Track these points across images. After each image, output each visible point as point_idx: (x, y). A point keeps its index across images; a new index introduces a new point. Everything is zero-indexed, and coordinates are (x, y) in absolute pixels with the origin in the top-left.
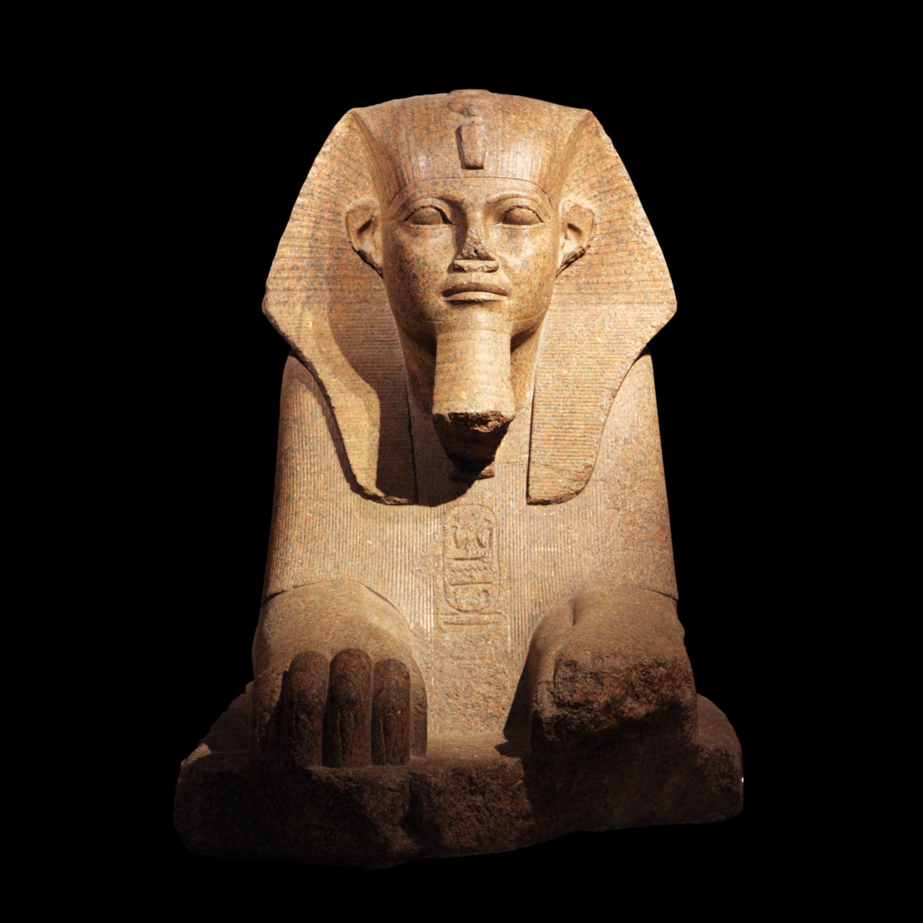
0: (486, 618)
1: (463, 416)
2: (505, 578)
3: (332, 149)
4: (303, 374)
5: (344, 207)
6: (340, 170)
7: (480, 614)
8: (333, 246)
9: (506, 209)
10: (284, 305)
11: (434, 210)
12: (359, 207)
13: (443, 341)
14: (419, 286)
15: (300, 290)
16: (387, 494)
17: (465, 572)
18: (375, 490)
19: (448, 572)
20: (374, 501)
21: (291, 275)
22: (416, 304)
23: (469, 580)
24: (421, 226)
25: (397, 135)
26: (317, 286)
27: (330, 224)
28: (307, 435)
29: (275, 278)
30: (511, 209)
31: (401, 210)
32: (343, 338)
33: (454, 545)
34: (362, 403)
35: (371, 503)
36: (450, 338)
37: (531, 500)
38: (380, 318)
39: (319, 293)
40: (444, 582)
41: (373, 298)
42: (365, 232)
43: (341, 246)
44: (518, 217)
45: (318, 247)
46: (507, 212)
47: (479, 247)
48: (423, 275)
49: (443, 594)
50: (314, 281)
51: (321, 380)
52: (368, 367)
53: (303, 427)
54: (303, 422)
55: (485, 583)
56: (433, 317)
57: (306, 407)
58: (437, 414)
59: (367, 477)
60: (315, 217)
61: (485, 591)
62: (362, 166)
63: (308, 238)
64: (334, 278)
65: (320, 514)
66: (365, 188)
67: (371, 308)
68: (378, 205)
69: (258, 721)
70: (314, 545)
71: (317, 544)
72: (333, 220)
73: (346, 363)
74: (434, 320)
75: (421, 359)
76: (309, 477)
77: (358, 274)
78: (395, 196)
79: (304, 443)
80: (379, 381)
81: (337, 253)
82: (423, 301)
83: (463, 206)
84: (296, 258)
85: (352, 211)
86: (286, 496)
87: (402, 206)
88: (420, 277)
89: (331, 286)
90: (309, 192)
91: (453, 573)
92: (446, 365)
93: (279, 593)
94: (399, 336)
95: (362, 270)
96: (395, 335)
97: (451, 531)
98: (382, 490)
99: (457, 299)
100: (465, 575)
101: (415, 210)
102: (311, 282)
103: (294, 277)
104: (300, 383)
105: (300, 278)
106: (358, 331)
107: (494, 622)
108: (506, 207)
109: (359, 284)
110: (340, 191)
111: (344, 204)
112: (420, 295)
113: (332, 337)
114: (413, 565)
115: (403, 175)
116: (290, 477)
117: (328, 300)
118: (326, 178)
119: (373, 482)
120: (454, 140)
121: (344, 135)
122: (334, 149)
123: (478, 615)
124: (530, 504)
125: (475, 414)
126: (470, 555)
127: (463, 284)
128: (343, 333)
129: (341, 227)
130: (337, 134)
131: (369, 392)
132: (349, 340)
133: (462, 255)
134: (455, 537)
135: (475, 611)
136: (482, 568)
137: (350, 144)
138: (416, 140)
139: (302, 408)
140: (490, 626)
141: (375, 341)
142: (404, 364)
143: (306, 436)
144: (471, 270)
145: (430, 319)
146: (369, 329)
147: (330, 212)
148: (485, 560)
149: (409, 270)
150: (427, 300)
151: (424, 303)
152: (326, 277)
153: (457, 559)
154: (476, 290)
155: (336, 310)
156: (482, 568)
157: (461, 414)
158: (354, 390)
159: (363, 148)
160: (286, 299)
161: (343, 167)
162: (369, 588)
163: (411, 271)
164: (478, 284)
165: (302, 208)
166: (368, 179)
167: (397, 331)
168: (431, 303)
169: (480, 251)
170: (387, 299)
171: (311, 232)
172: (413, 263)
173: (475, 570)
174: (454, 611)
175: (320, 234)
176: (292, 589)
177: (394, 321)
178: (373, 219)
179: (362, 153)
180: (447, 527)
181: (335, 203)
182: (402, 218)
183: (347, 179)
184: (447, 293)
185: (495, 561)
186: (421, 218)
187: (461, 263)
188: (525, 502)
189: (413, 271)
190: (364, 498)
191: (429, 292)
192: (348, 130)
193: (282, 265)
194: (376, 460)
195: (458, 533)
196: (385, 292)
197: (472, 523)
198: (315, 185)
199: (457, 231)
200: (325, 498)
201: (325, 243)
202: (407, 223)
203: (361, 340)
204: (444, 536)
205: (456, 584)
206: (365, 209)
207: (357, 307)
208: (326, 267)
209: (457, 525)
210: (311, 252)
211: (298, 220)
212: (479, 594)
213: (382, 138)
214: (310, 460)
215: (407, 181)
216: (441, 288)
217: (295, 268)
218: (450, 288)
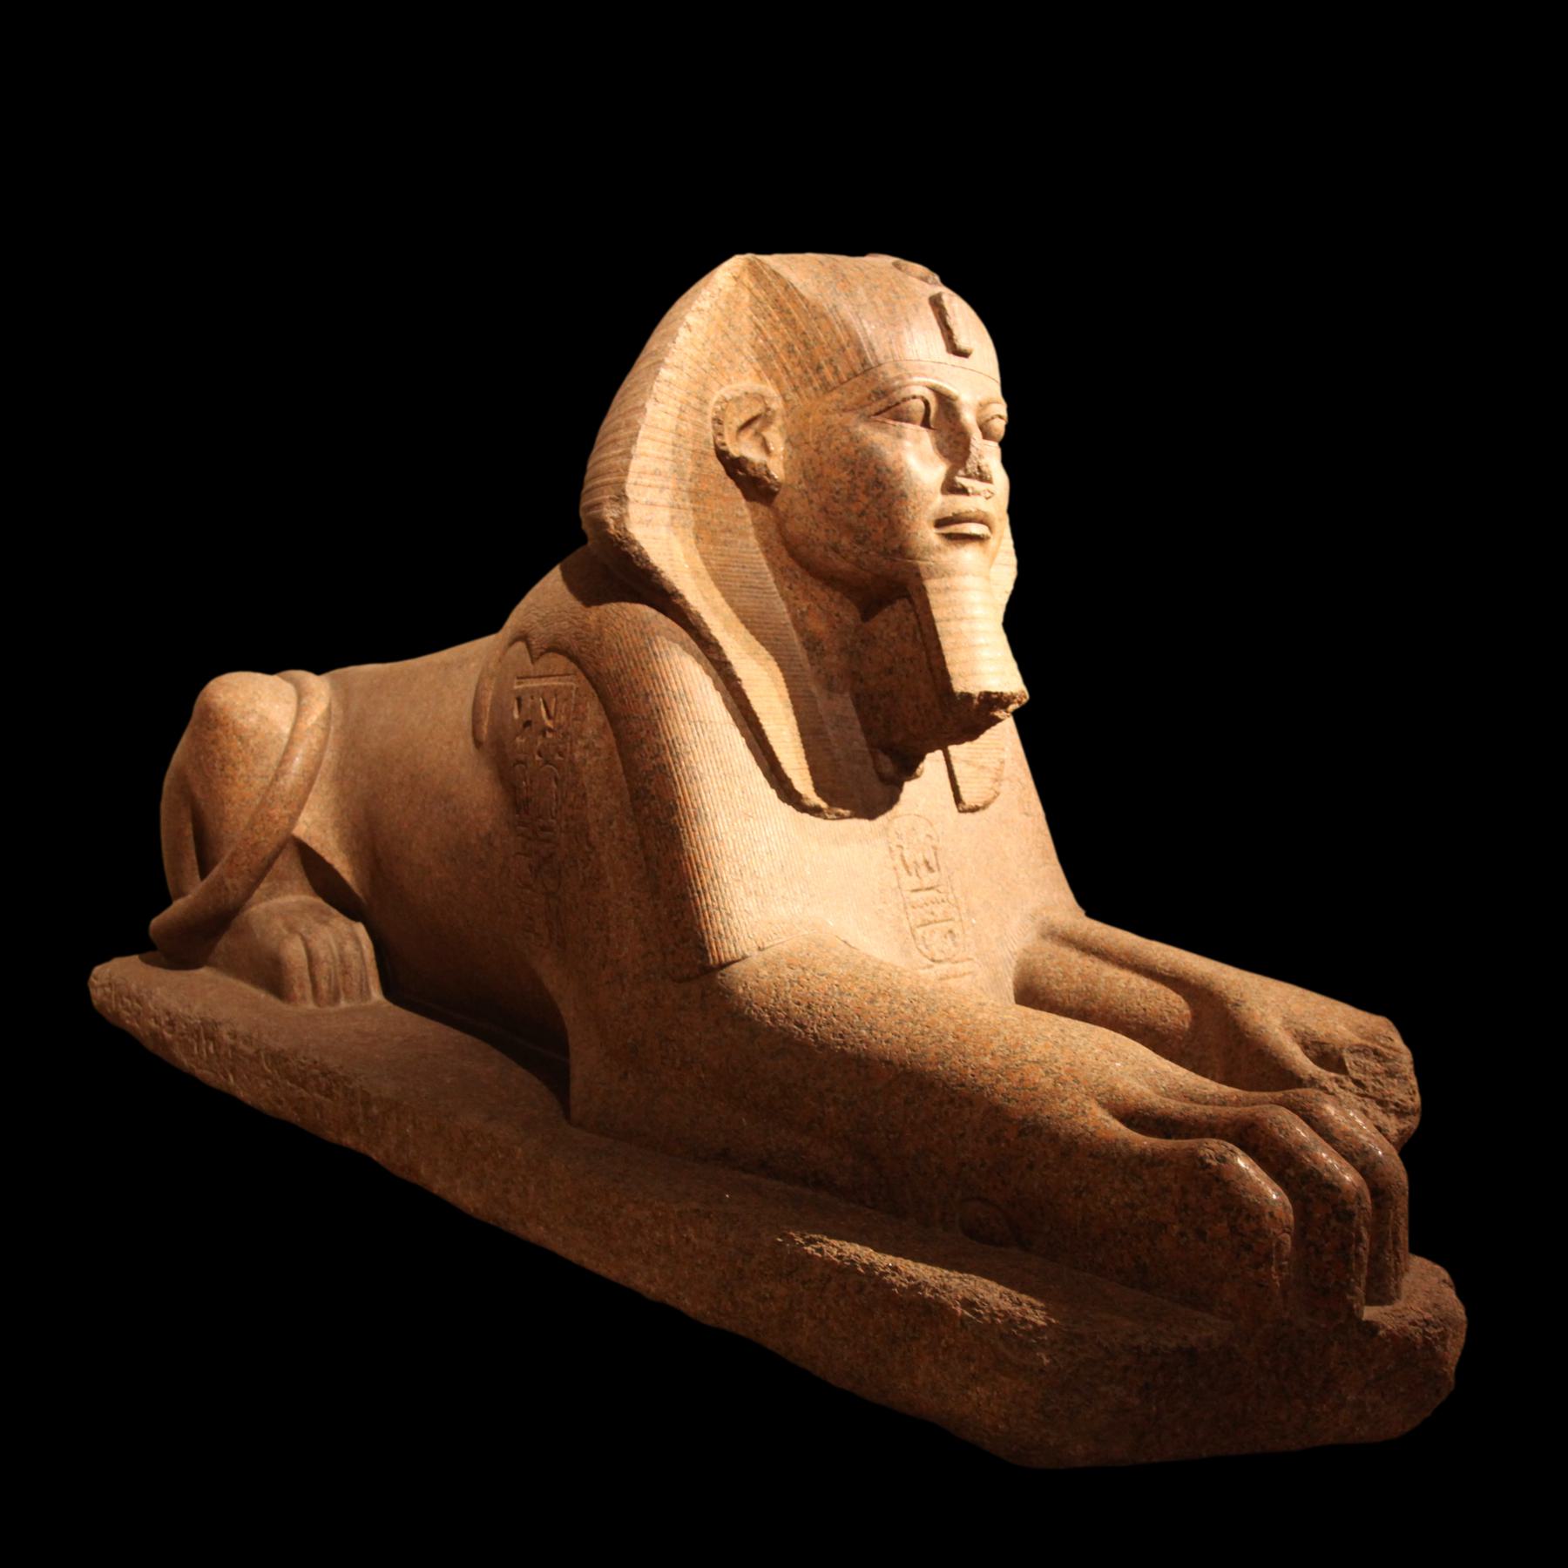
0: (960, 967)
1: (995, 696)
2: (965, 911)
3: (711, 306)
4: (670, 630)
5: (713, 393)
6: (716, 338)
7: (953, 963)
8: (696, 448)
9: (989, 417)
10: (647, 525)
11: (922, 405)
12: (746, 393)
13: (939, 591)
14: (907, 509)
15: (663, 506)
16: (830, 804)
17: (925, 907)
18: (814, 799)
19: (910, 910)
20: (811, 814)
21: (653, 482)
22: (895, 535)
23: (931, 918)
24: (904, 424)
25: (851, 294)
26: (680, 503)
27: (695, 414)
28: (702, 719)
29: (635, 484)
30: (993, 418)
31: (874, 398)
32: (720, 580)
33: (905, 872)
34: (766, 673)
35: (806, 816)
36: (949, 586)
37: (966, 807)
38: (746, 555)
39: (683, 512)
40: (910, 924)
41: (736, 527)
42: (742, 433)
43: (704, 449)
44: (996, 430)
45: (680, 446)
46: (988, 421)
47: (983, 462)
48: (915, 494)
49: (913, 941)
50: (677, 494)
51: (715, 639)
52: (755, 622)
53: (693, 708)
54: (690, 699)
55: (947, 920)
56: (919, 555)
57: (689, 678)
58: (962, 693)
59: (802, 781)
60: (681, 402)
61: (951, 932)
62: (741, 338)
63: (671, 431)
64: (696, 493)
65: (750, 838)
66: (742, 371)
67: (736, 542)
68: (776, 395)
69: (1274, 1251)
70: (757, 884)
71: (759, 883)
72: (699, 410)
73: (734, 616)
74: (919, 559)
75: (837, 615)
76: (719, 781)
77: (720, 491)
78: (849, 379)
79: (700, 730)
80: (773, 644)
81: (698, 455)
82: (909, 531)
83: (957, 404)
84: (659, 458)
85: (738, 399)
86: (691, 811)
87: (876, 393)
88: (910, 495)
89: (696, 506)
90: (680, 364)
91: (914, 910)
92: (953, 623)
93: (738, 961)
94: (775, 582)
95: (724, 487)
96: (768, 581)
97: (897, 852)
98: (824, 799)
99: (959, 531)
100: (927, 912)
101: (905, 400)
102: (674, 496)
103: (657, 487)
104: (670, 642)
105: (662, 488)
106: (731, 571)
107: (970, 973)
108: (987, 415)
109: (721, 506)
110: (713, 369)
111: (714, 390)
112: (907, 522)
113: (709, 578)
114: (874, 903)
115: (873, 350)
116: (691, 782)
117: (693, 524)
118: (700, 347)
119: (811, 789)
120: (930, 313)
121: (728, 289)
122: (714, 307)
123: (952, 965)
124: (960, 811)
125: (1009, 694)
126: (926, 883)
127: (971, 512)
128: (718, 572)
129: (706, 421)
130: (721, 287)
131: (768, 659)
132: (727, 583)
133: (966, 471)
134: (904, 861)
135: (948, 960)
136: (940, 901)
137: (733, 304)
138: (886, 303)
139: (684, 679)
140: (968, 978)
141: (751, 587)
142: (789, 621)
143: (701, 722)
144: (977, 494)
145: (912, 558)
146: (741, 569)
147: (697, 397)
148: (939, 888)
149: (893, 484)
150: (915, 530)
151: (909, 534)
152: (690, 491)
153: (916, 891)
154: (982, 522)
155: (702, 539)
156: (940, 901)
157: (996, 693)
158: (754, 654)
159: (749, 312)
160: (649, 518)
161: (719, 336)
162: (845, 942)
163: (898, 485)
164: (986, 514)
165: (669, 386)
166: (746, 358)
167: (769, 575)
168: (919, 534)
169: (984, 469)
170: (751, 530)
171: (675, 423)
172: (902, 474)
173: (933, 903)
174: (931, 963)
175: (684, 428)
176: (756, 953)
177: (763, 561)
178: (770, 413)
179: (744, 321)
180: (894, 848)
181: (704, 385)
182: (870, 410)
183: (722, 353)
184: (940, 523)
185: (950, 890)
186: (908, 412)
187: (962, 481)
188: (956, 809)
189: (901, 487)
190: (798, 810)
191: (920, 519)
192: (733, 283)
193: (644, 467)
194: (803, 755)
195: (906, 855)
196: (749, 520)
197: (915, 841)
198: (686, 354)
199: (936, 437)
200: (750, 814)
201: (688, 442)
202: (879, 418)
203: (738, 584)
204: (893, 859)
205: (922, 925)
206: (756, 398)
207: (722, 538)
208: (688, 477)
209: (902, 844)
210: (673, 452)
211: (663, 403)
212: (945, 937)
213: (821, 295)
214: (715, 756)
215: (881, 359)
216: (934, 514)
217: (658, 472)
218: (951, 515)
